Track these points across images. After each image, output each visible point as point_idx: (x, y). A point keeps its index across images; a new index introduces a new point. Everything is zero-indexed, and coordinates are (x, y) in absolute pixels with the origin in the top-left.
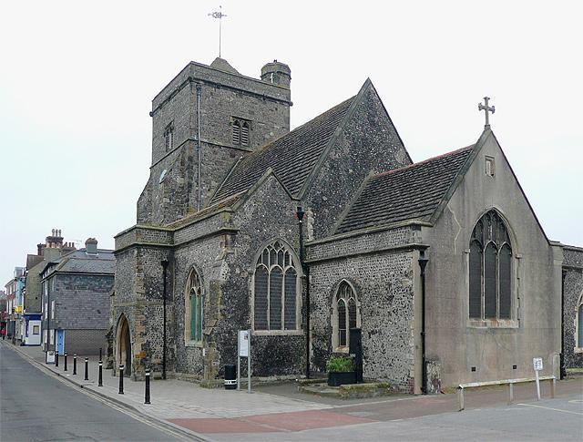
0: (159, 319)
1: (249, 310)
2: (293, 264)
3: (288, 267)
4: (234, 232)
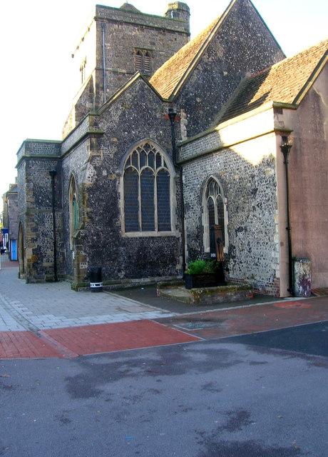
0: (48, 225)
1: (118, 212)
2: (165, 165)
3: (160, 168)
4: (100, 135)
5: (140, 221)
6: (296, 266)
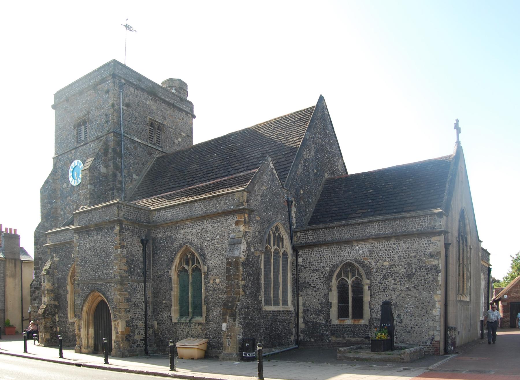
0: (140, 296)
1: (260, 288)
2: (286, 248)
3: (283, 250)
4: (251, 211)
5: (272, 295)
6: (448, 332)
